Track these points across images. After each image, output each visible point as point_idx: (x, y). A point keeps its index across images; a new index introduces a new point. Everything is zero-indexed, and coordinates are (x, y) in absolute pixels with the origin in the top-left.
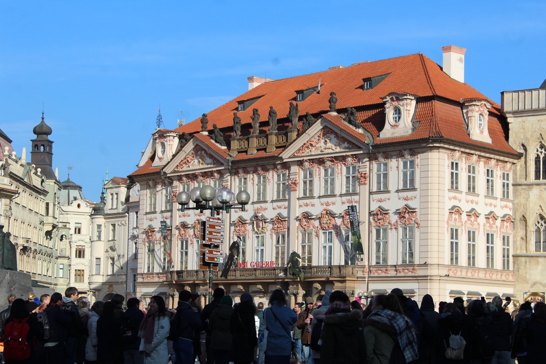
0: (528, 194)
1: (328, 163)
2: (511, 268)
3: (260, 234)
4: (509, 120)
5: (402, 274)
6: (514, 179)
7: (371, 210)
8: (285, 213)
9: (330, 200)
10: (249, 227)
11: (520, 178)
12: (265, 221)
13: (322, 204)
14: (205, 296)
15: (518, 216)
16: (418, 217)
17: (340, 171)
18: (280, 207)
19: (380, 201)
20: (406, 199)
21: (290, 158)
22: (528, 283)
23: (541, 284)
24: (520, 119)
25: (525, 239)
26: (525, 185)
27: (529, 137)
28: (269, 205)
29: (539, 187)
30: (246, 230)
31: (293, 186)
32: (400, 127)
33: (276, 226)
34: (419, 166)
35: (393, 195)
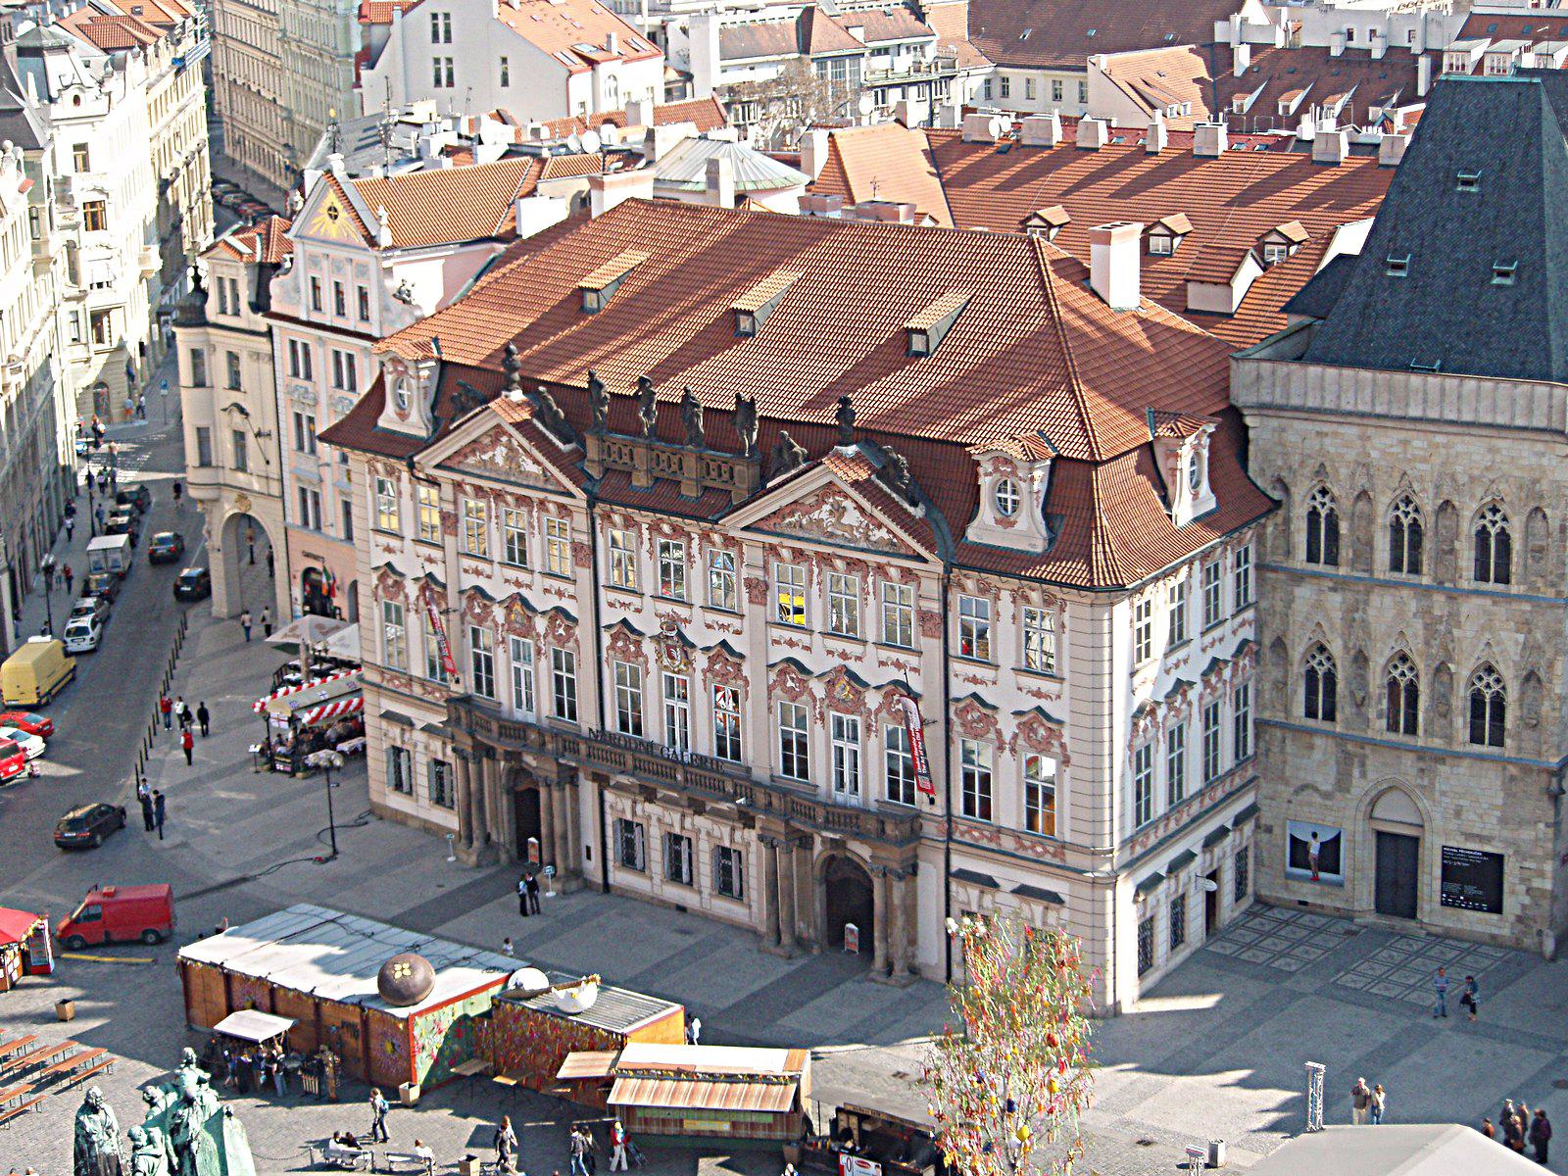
0: (1292, 593)
2: (1250, 751)
3: (678, 673)
4: (1249, 421)
5: (1030, 854)
6: (1259, 555)
7: (954, 693)
11: (1273, 553)
13: (830, 652)
14: (548, 786)
15: (1267, 641)
17: (871, 590)
19: (975, 680)
20: (1038, 694)
21: (746, 529)
22: (1287, 783)
23: (1316, 789)
24: (1274, 423)
25: (1281, 685)
26: (1286, 570)
27: (1296, 466)
29: (1315, 581)
30: (639, 653)
32: (1016, 527)
34: (1067, 630)
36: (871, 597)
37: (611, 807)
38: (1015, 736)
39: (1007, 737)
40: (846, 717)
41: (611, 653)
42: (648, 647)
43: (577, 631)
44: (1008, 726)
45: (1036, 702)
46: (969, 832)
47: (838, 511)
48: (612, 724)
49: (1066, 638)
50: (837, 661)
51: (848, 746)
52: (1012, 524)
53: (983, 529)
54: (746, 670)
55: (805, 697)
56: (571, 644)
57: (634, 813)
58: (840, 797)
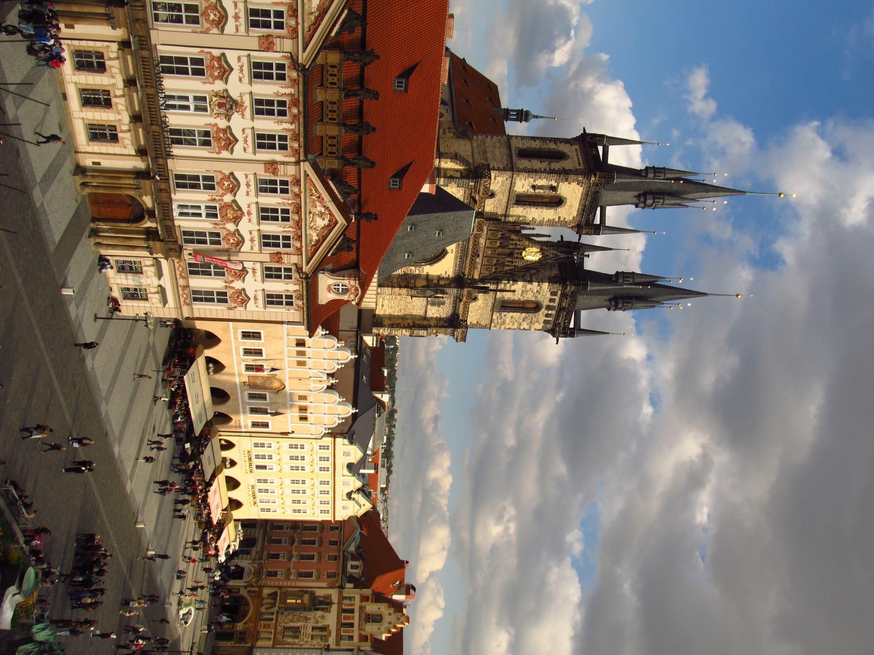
1: (296, 218)
5: (181, 292)
8: (238, 151)
9: (254, 217)
10: (219, 86)
12: (228, 118)
13: (249, 206)
16: (239, 308)
18: (246, 141)
20: (256, 298)
21: (305, 172)
28: (247, 123)
30: (215, 78)
31: (271, 170)
33: (221, 135)
35: (260, 286)
36: (282, 229)
37: (108, 46)
38: (233, 288)
39: (232, 285)
40: (218, 212)
41: (209, 56)
42: (219, 86)
43: (215, 31)
44: (238, 285)
45: (252, 296)
46: (180, 266)
47: (321, 215)
48: (164, 50)
49: (284, 310)
50: (245, 210)
51: (203, 211)
52: (329, 291)
53: (325, 281)
54: (225, 154)
55: (221, 192)
56: (206, 25)
57: (112, 67)
58: (175, 206)
